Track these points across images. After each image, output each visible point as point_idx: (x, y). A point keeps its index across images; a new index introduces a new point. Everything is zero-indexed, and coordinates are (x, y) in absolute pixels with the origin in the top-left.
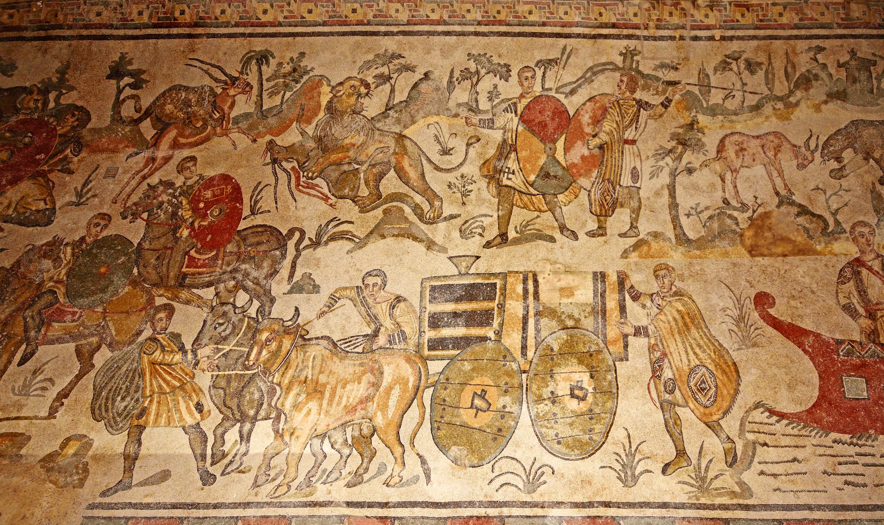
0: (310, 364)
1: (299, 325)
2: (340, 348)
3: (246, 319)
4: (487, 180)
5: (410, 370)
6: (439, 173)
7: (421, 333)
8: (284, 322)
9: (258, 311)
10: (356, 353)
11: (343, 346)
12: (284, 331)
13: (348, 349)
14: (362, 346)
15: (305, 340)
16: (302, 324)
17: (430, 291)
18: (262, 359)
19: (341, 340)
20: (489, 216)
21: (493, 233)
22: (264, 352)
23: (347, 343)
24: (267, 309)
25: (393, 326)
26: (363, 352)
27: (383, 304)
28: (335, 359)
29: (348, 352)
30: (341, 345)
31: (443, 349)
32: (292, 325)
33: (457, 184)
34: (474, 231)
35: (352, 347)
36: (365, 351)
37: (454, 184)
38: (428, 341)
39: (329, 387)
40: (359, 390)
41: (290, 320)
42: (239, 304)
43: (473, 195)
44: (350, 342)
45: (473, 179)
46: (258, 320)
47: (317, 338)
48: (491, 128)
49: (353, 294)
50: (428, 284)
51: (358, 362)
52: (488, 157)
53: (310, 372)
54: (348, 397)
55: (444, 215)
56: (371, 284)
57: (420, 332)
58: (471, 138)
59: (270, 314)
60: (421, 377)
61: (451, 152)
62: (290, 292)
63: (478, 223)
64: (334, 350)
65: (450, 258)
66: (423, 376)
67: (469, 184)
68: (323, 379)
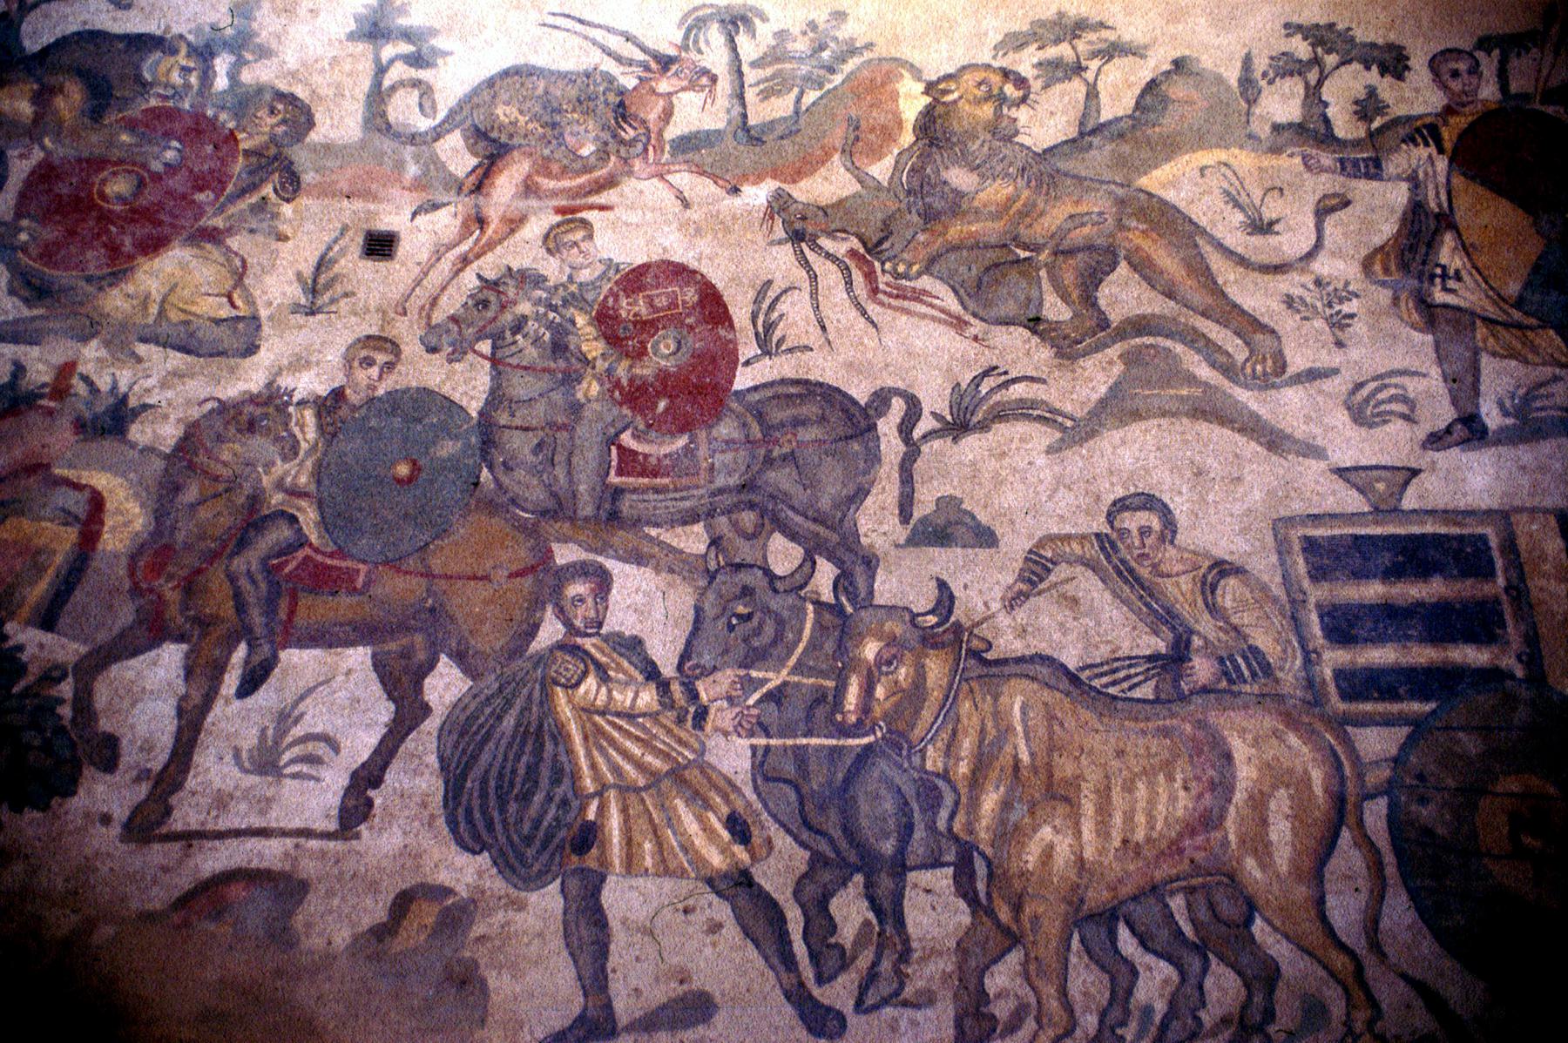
1: (958, 628)
3: (810, 607)
7: (1310, 658)
8: (914, 616)
10: (1138, 700)
12: (924, 640)
13: (1111, 690)
14: (1152, 683)
16: (966, 623)
18: (877, 711)
20: (1416, 373)
21: (1442, 413)
22: (880, 692)
24: (861, 582)
26: (1157, 701)
27: (1182, 579)
29: (1114, 698)
30: (1090, 679)
32: (938, 625)
33: (1308, 300)
34: (1387, 407)
35: (1125, 685)
37: (1301, 298)
42: (781, 568)
47: (1020, 660)
49: (1093, 551)
50: (1296, 534)
52: (1377, 240)
54: (1151, 818)
55: (1291, 370)
57: (1306, 653)
58: (1325, 196)
59: (871, 593)
61: (1277, 228)
62: (912, 541)
63: (1393, 391)
64: (1076, 692)
66: (1348, 770)
67: (1341, 302)
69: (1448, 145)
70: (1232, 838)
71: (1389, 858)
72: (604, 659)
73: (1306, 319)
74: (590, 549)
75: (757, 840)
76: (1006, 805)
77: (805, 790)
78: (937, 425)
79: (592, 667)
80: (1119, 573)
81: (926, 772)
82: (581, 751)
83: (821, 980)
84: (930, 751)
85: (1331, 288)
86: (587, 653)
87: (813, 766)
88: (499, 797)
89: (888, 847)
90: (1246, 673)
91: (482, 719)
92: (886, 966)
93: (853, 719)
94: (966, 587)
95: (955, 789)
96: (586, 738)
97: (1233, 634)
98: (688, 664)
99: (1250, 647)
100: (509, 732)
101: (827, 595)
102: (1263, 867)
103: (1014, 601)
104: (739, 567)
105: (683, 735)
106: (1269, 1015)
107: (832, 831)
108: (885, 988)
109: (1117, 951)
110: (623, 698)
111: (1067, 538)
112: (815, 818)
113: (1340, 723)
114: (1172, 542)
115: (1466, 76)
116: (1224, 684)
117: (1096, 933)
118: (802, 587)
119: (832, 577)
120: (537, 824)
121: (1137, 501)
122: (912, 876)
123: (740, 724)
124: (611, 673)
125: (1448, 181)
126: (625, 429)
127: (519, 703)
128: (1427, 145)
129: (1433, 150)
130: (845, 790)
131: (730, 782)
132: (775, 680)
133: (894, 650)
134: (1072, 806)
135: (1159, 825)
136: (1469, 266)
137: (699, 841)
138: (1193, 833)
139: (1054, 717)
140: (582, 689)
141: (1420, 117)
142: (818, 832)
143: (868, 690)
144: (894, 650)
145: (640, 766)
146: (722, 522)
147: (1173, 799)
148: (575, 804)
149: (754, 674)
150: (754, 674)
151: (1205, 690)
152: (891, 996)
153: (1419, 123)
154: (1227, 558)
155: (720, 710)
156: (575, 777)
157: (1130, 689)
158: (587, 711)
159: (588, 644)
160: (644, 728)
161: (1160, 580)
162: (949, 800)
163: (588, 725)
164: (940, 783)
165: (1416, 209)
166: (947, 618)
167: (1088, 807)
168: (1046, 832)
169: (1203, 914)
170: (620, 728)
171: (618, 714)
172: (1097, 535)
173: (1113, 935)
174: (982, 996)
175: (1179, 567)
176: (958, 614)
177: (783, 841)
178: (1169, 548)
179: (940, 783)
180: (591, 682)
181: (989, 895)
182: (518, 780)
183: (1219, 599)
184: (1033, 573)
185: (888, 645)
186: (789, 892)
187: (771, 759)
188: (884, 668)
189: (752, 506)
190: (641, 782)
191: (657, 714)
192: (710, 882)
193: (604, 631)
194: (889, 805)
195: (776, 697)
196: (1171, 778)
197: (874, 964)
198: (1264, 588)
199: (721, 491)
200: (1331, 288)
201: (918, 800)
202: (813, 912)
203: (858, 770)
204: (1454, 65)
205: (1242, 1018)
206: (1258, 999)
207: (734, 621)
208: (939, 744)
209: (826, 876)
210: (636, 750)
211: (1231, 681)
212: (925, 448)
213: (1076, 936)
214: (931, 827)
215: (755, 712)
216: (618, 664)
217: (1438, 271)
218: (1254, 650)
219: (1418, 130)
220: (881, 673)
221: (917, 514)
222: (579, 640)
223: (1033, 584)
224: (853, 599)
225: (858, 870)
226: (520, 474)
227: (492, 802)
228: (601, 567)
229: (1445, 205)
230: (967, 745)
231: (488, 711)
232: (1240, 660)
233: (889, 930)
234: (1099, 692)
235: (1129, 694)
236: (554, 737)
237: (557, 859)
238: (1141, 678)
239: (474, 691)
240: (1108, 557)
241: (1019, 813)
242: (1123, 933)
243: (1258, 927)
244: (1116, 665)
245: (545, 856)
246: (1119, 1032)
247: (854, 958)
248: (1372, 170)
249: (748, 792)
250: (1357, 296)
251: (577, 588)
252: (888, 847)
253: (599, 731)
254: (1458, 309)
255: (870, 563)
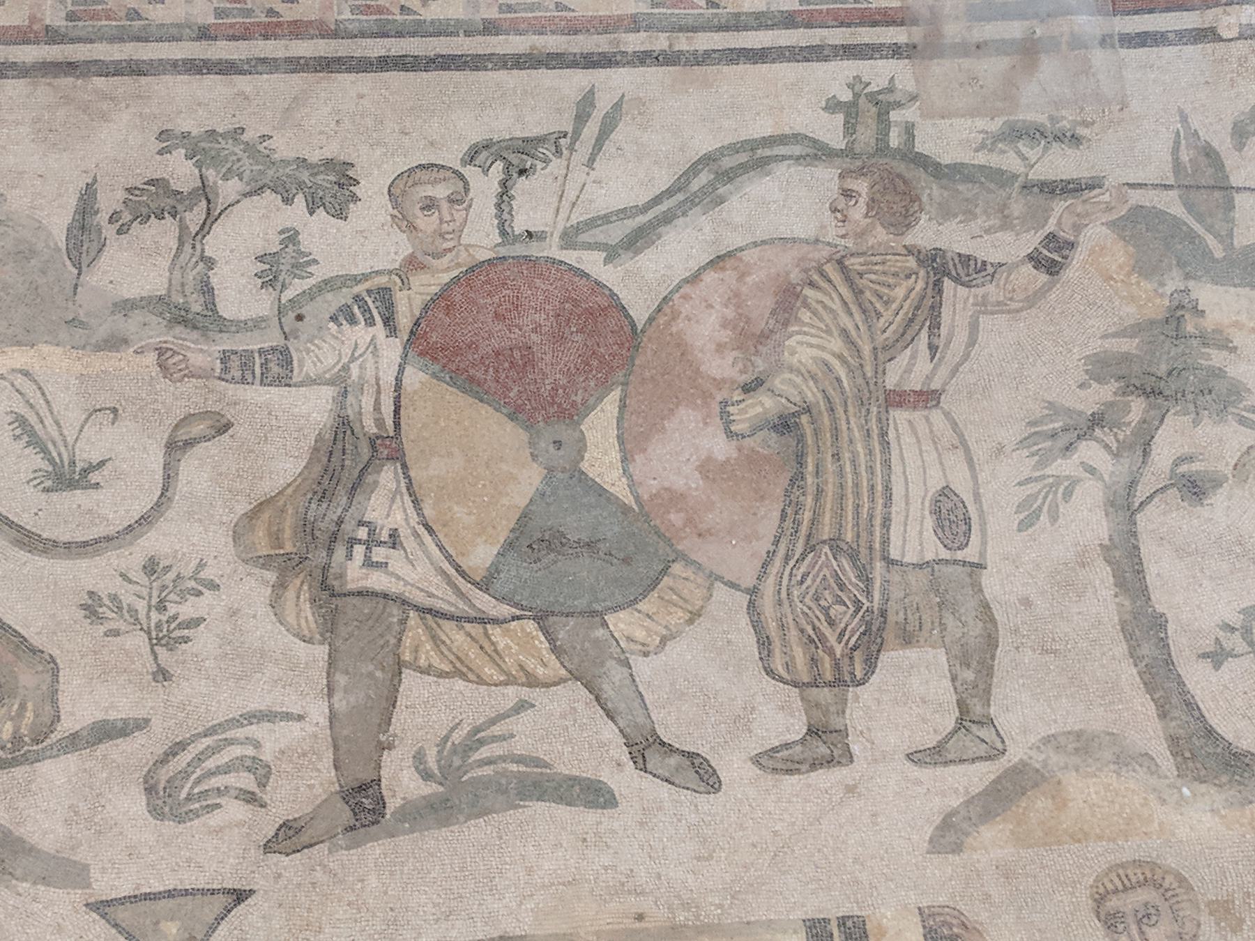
4: (271, 576)
6: (40, 561)
33: (127, 599)
37: (114, 598)
43: (204, 642)
45: (202, 575)
48: (284, 381)
67: (183, 595)
69: (404, 321)
73: (116, 633)
85: (171, 575)
115: (445, 205)
125: (399, 380)
128: (370, 322)
129: (379, 330)
136: (414, 519)
141: (366, 277)
153: (360, 289)
165: (344, 426)
200: (171, 575)
204: (429, 191)
217: (362, 533)
219: (357, 298)
229: (389, 422)
248: (275, 369)
250: (214, 586)
254: (385, 596)
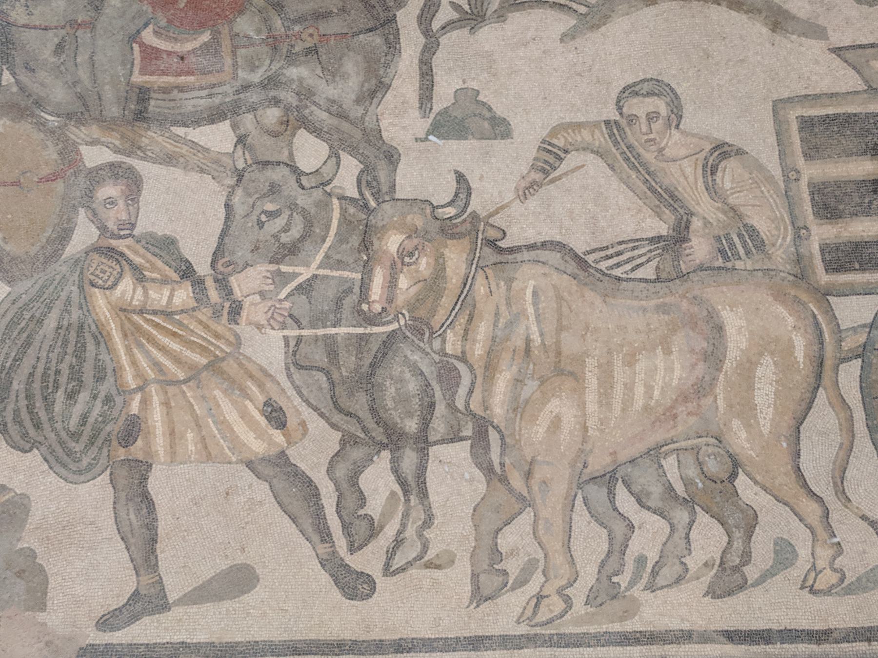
0: (531, 310)
1: (475, 216)
2: (597, 270)
3: (335, 201)
5: (791, 320)
7: (800, 232)
8: (434, 208)
9: (359, 182)
11: (603, 265)
12: (442, 230)
13: (618, 272)
14: (654, 263)
15: (501, 251)
16: (483, 214)
17: (801, 130)
18: (400, 299)
19: (594, 251)
22: (403, 282)
23: (610, 257)
24: (382, 175)
25: (721, 216)
26: (658, 280)
28: (590, 295)
29: (619, 279)
30: (596, 262)
31: (863, 269)
32: (457, 216)
35: (628, 267)
36: (664, 276)
38: (822, 250)
39: (591, 363)
40: (672, 370)
41: (450, 204)
44: (618, 254)
46: (366, 206)
47: (532, 247)
49: (601, 139)
50: (793, 114)
51: (653, 303)
53: (534, 328)
54: (649, 389)
56: (641, 112)
57: (797, 229)
59: (393, 187)
60: (821, 334)
64: (581, 274)
65: (837, 51)
66: (826, 336)
68: (570, 344)
70: (720, 403)
71: (859, 415)
72: (138, 260)
74: (117, 151)
75: (292, 422)
76: (518, 382)
77: (336, 376)
78: (455, 15)
79: (127, 268)
80: (627, 159)
81: (446, 355)
82: (122, 352)
83: (353, 548)
84: (450, 335)
86: (122, 254)
87: (343, 354)
88: (45, 398)
89: (412, 425)
90: (742, 252)
91: (23, 324)
92: (410, 532)
93: (377, 308)
94: (481, 178)
95: (471, 368)
96: (125, 336)
97: (731, 214)
98: (221, 262)
99: (745, 225)
100: (51, 335)
101: (353, 192)
102: (748, 426)
103: (528, 190)
104: (266, 164)
105: (219, 329)
106: (746, 557)
107: (361, 414)
108: (409, 552)
109: (615, 509)
110: (159, 297)
111: (577, 126)
112: (344, 402)
113: (824, 294)
114: (677, 126)
116: (720, 262)
117: (598, 494)
118: (328, 182)
119: (356, 172)
120: (84, 419)
121: (646, 87)
122: (433, 450)
123: (272, 317)
124: (146, 273)
126: (146, 25)
127: (59, 305)
130: (372, 375)
131: (267, 374)
132: (305, 274)
133: (416, 241)
134: (577, 380)
135: (656, 393)
137: (241, 429)
138: (686, 399)
139: (562, 298)
140: (120, 288)
142: (349, 414)
143: (392, 284)
144: (416, 241)
145: (177, 360)
146: (248, 120)
147: (670, 369)
148: (119, 400)
149: (284, 268)
150: (284, 268)
151: (701, 268)
152: (415, 559)
154: (727, 140)
155: (252, 304)
156: (117, 371)
157: (633, 270)
158: (123, 310)
159: (121, 245)
160: (180, 324)
161: (663, 165)
162: (466, 381)
163: (127, 325)
164: (461, 366)
166: (464, 210)
167: (592, 381)
168: (554, 406)
169: (692, 472)
170: (157, 326)
171: (155, 313)
172: (607, 123)
173: (612, 496)
174: (496, 554)
175: (683, 152)
176: (475, 204)
177: (316, 424)
178: (674, 131)
179: (461, 366)
180: (127, 284)
181: (502, 465)
182: (63, 380)
183: (718, 181)
184: (546, 162)
185: (409, 237)
186: (324, 470)
187: (304, 348)
188: (407, 260)
189: (276, 102)
190: (181, 376)
191: (194, 309)
192: (249, 465)
193: (136, 232)
194: (413, 386)
195: (305, 288)
196: (668, 352)
197: (400, 532)
198: (761, 168)
199: (246, 87)
201: (440, 381)
202: (345, 485)
203: (385, 354)
205: (722, 563)
206: (738, 544)
207: (263, 218)
208: (458, 328)
209: (356, 454)
210: (175, 346)
211: (726, 258)
212: (443, 40)
213: (579, 498)
214: (451, 406)
215: (287, 305)
216: (152, 264)
218: (752, 231)
220: (403, 263)
221: (437, 108)
222: (114, 243)
223: (546, 173)
224: (376, 195)
225: (384, 446)
226: (42, 75)
227: (39, 403)
228: (131, 168)
230: (483, 330)
231: (27, 315)
232: (736, 240)
233: (414, 500)
234: (604, 274)
235: (632, 276)
236: (95, 338)
237: (105, 451)
238: (644, 259)
239: (13, 297)
240: (616, 143)
241: (531, 387)
242: (621, 492)
243: (742, 481)
244: (623, 246)
245: (95, 449)
246: (615, 579)
247: (382, 528)
249: (282, 378)
251: (109, 190)
252: (412, 425)
253: (138, 328)
255: (392, 157)
